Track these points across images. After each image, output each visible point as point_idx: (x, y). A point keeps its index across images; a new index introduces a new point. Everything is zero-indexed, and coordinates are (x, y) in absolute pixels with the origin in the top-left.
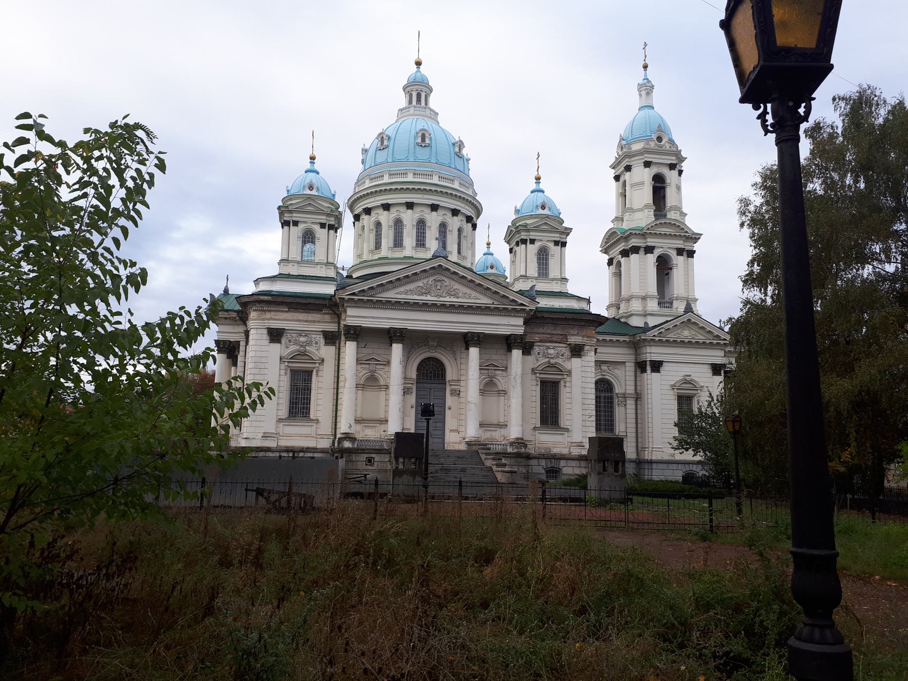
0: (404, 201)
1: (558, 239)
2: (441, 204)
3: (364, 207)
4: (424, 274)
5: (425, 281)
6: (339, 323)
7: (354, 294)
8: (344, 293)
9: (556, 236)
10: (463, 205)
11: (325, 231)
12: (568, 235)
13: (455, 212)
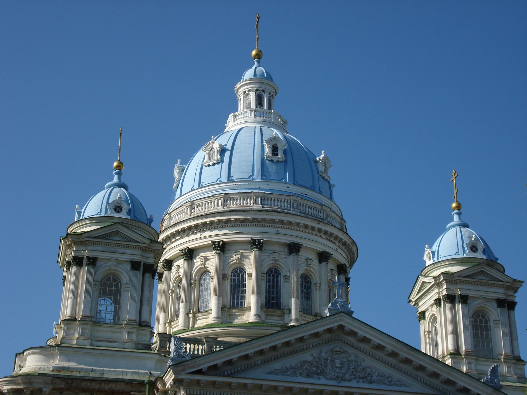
1: (502, 297)
4: (316, 340)
5: (315, 352)
7: (199, 372)
8: (183, 370)
9: (499, 293)
10: (335, 247)
11: (138, 275)
12: (516, 291)
13: (323, 257)
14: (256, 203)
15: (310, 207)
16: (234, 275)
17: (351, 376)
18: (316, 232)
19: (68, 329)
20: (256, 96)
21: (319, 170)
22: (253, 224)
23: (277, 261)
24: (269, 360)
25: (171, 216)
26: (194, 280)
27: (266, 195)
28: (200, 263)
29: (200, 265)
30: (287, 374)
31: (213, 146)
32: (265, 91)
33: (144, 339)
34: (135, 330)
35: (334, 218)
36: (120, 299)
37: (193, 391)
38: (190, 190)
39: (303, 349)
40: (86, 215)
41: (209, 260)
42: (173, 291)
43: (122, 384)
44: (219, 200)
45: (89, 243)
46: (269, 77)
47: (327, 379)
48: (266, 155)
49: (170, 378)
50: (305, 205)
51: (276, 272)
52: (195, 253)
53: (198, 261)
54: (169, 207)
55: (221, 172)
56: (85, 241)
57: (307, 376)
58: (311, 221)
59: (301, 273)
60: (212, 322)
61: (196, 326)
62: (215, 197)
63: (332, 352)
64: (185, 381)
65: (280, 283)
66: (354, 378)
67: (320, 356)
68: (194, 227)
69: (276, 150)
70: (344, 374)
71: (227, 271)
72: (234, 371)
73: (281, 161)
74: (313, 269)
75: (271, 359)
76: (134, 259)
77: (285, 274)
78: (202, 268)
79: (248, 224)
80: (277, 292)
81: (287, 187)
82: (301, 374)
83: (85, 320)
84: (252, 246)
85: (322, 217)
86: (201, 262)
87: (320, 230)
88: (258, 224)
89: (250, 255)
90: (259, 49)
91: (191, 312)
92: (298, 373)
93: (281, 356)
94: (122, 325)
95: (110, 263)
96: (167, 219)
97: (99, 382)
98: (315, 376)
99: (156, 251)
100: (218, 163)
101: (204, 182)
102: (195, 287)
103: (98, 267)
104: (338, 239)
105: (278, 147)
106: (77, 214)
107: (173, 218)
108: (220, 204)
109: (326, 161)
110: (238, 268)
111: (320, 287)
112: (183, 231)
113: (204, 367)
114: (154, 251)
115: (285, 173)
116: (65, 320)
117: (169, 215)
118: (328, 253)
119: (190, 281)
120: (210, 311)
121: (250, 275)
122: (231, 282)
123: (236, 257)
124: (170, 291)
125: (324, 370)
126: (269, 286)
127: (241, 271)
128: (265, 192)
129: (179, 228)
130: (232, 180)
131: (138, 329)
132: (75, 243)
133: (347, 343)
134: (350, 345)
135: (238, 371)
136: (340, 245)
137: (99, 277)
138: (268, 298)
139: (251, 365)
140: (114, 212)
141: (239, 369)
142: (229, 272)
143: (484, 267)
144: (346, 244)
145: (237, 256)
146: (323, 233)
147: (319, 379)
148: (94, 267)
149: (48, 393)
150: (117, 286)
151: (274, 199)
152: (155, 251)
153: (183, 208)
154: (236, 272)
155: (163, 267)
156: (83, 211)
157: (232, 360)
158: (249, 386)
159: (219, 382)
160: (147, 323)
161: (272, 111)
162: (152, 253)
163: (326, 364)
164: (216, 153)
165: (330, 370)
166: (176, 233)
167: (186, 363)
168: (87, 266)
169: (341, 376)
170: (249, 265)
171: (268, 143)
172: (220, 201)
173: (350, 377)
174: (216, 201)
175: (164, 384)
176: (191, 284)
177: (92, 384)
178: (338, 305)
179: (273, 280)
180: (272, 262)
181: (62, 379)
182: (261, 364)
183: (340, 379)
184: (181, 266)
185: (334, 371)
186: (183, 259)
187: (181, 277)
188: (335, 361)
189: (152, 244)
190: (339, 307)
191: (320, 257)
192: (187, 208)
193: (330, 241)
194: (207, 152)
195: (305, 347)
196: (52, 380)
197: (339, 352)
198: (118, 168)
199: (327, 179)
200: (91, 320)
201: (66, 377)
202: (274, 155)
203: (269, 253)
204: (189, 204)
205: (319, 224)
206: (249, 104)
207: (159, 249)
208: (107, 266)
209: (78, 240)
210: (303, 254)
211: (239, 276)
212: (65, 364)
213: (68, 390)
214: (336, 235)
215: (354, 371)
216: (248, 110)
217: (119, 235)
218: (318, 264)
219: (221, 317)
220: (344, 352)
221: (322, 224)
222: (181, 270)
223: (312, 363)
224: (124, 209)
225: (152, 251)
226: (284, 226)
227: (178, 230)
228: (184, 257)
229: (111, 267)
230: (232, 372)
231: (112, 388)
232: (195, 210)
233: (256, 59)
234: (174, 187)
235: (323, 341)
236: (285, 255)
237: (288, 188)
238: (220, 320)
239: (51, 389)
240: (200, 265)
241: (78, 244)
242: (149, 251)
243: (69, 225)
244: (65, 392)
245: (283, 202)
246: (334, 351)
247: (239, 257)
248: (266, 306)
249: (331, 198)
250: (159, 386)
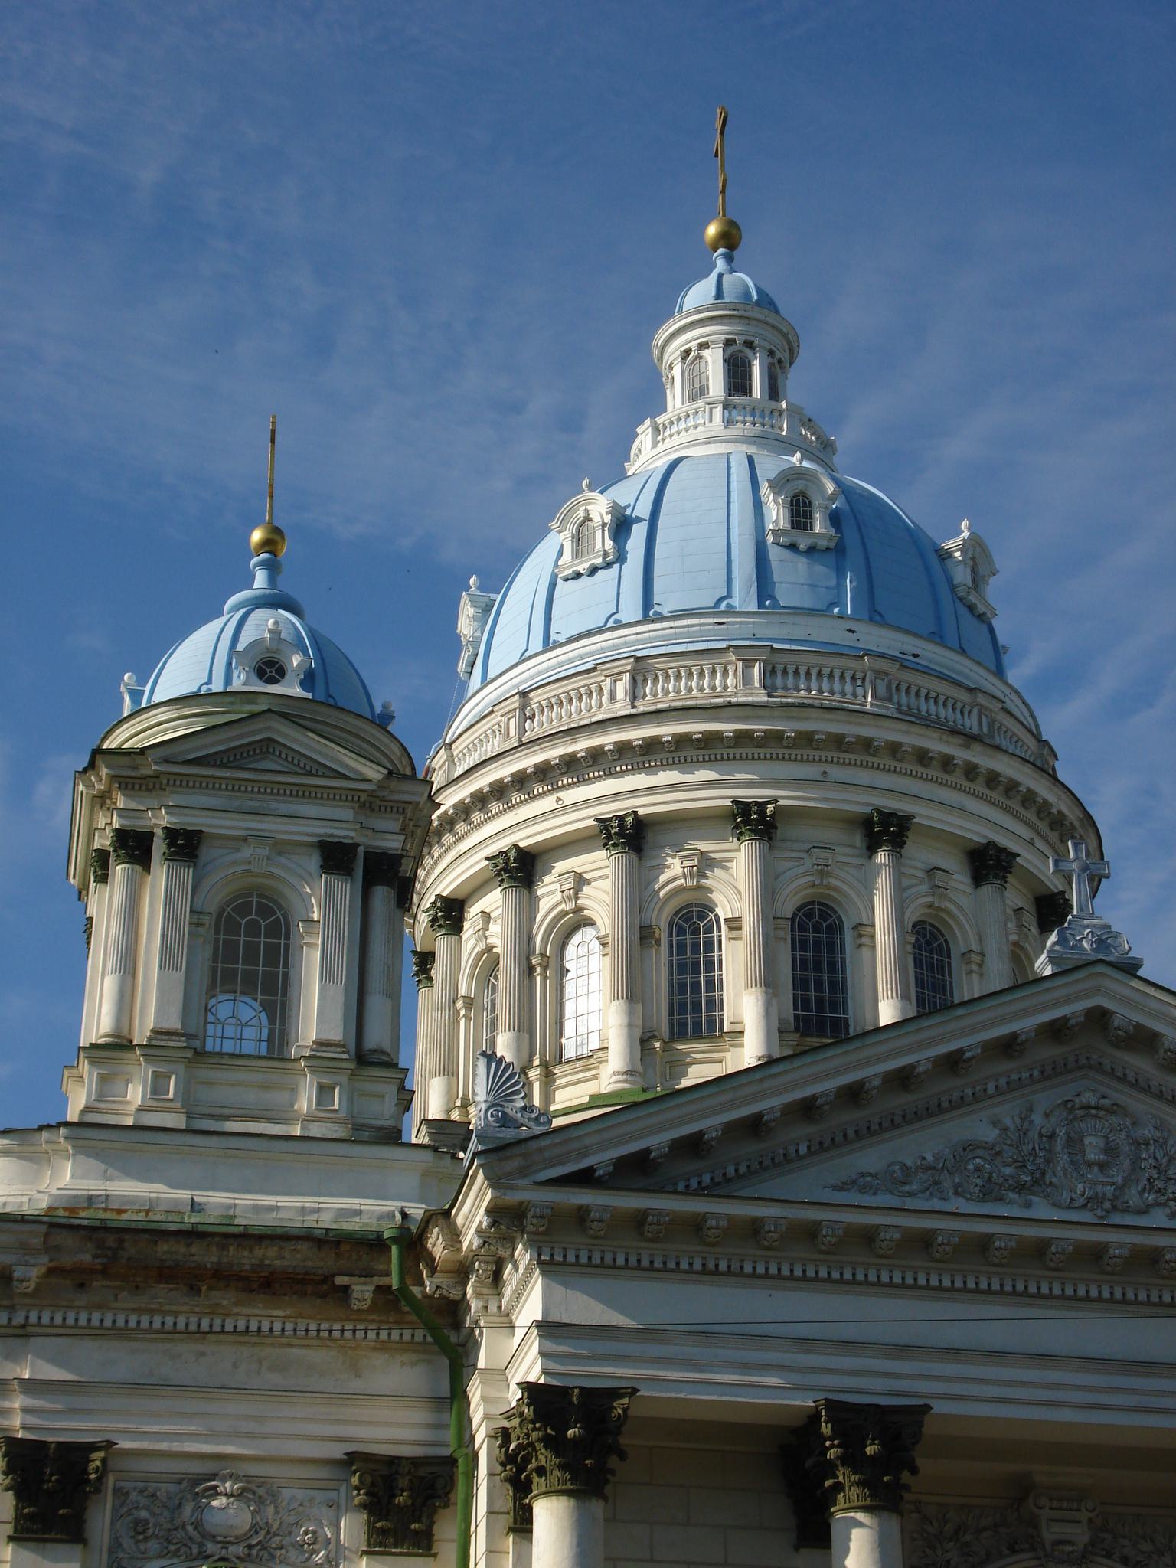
0: (720, 799)
2: (924, 815)
3: (493, 849)
5: (1008, 1112)
6: (458, 1396)
7: (584, 1178)
8: (523, 1172)
14: (746, 681)
15: (933, 694)
16: (681, 931)
17: (1146, 1195)
19: (103, 1079)
20: (725, 361)
21: (955, 582)
22: (738, 751)
23: (828, 874)
24: (839, 1138)
25: (455, 753)
26: (543, 955)
27: (777, 657)
28: (558, 897)
29: (559, 904)
30: (907, 1188)
31: (587, 511)
32: (755, 344)
33: (382, 1110)
34: (344, 1079)
35: (1016, 739)
36: (286, 975)
37: (565, 1249)
38: (517, 660)
39: (962, 1098)
40: (157, 698)
41: (588, 882)
42: (469, 1002)
43: (303, 1247)
44: (615, 681)
45: (171, 782)
46: (766, 302)
47: (1056, 1205)
48: (771, 527)
49: (474, 1208)
50: (914, 690)
51: (824, 915)
52: (539, 866)
53: (553, 892)
54: (446, 729)
55: (618, 594)
56: (157, 776)
57: (984, 1195)
59: (914, 919)
60: (610, 1086)
61: (553, 1108)
62: (601, 670)
63: (1071, 1110)
64: (531, 1213)
65: (843, 952)
66: (1159, 1205)
67: (1026, 1125)
68: (535, 773)
69: (805, 512)
70: (1121, 1188)
71: (654, 916)
72: (712, 1179)
73: (824, 548)
75: (845, 1135)
76: (331, 836)
77: (855, 921)
78: (567, 913)
79: (719, 751)
80: (833, 986)
81: (849, 630)
82: (959, 1189)
83: (162, 1043)
84: (737, 827)
85: (975, 730)
86: (563, 892)
87: (971, 771)
88: (756, 751)
89: (731, 860)
90: (732, 215)
91: (536, 1062)
92: (947, 1184)
93: (880, 1124)
94: (297, 1060)
95: (247, 852)
96: (440, 768)
97: (217, 1239)
98: (1012, 1195)
99: (409, 810)
100: (608, 565)
101: (561, 629)
102: (545, 978)
103: (204, 866)
104: (1035, 802)
105: (810, 502)
106: (127, 699)
107: (459, 759)
108: (620, 694)
109: (976, 549)
110: (690, 905)
111: (980, 965)
112: (498, 791)
113: (601, 1159)
114: (400, 808)
115: (841, 576)
116: (94, 1046)
117: (448, 751)
118: (1005, 849)
119: (529, 961)
120: (601, 1054)
121: (734, 924)
122: (671, 954)
123: (684, 868)
124: (460, 1004)
125: (1043, 1174)
126: (804, 963)
127: (702, 916)
128: (775, 646)
129: (482, 781)
130: (657, 613)
131: (352, 1075)
132: (126, 783)
133: (1123, 1079)
134: (1135, 1085)
135: (729, 1181)
136: (1043, 826)
137: (213, 900)
138: (801, 1003)
139: (773, 1159)
140: (254, 678)
141: (731, 1171)
142: (661, 922)
144: (1062, 825)
145: (686, 863)
146: (981, 780)
147: (1028, 1205)
148: (192, 864)
149: (33, 1285)
150: (274, 930)
151: (808, 670)
152: (404, 809)
153: (492, 719)
154: (686, 921)
155: (432, 927)
156: (148, 689)
157: (704, 1134)
158: (772, 1228)
159: (660, 1212)
160: (387, 1054)
161: (784, 405)
162: (398, 816)
163: (1050, 1151)
164: (599, 533)
165: (1065, 1171)
166: (473, 803)
167: (533, 1145)
168: (166, 859)
169: (1109, 1196)
170: (731, 893)
171: (776, 490)
172: (621, 687)
173: (1142, 1198)
174: (607, 686)
175: (454, 1236)
176: (531, 969)
177: (193, 1250)
178: (1081, 939)
179: (817, 944)
180: (810, 879)
181: (83, 1232)
182: (811, 1152)
183: (1107, 1205)
184: (493, 915)
185: (1083, 1175)
186: (500, 889)
187: (494, 950)
188: (1082, 1140)
189: (394, 784)
190: (1085, 944)
191: (977, 864)
192: (509, 719)
193: (1007, 810)
194: (567, 533)
195: (969, 1091)
196: (47, 1235)
197: (1096, 1108)
198: (267, 549)
199: (984, 614)
200: (185, 1044)
201: (98, 1223)
202: (798, 528)
203: (799, 851)
204: (516, 702)
205: (969, 748)
206: (703, 390)
207: (418, 800)
208: (234, 863)
209: (133, 774)
210: (919, 853)
211: (696, 931)
212: (94, 1185)
213: (104, 1272)
214: (1029, 790)
215: (1158, 1178)
216: (701, 403)
217: (277, 753)
219: (642, 1071)
220: (1115, 1109)
221: (977, 747)
222: (496, 928)
223: (997, 1150)
224: (289, 672)
225: (395, 809)
226: (847, 756)
227: (480, 791)
228: (502, 881)
229: (249, 863)
230: (704, 1185)
231: (267, 1262)
232: (535, 721)
233: (721, 251)
234: (461, 667)
235: (1032, 1069)
236: (852, 856)
237: (853, 632)
238: (638, 1079)
239: (43, 1270)
240: (559, 904)
241: (133, 788)
242: (383, 809)
243: (102, 735)
244: (95, 1284)
245: (837, 679)
246: (1077, 1106)
247: (693, 867)
248: (797, 1030)
249: (999, 672)
250: (436, 1244)
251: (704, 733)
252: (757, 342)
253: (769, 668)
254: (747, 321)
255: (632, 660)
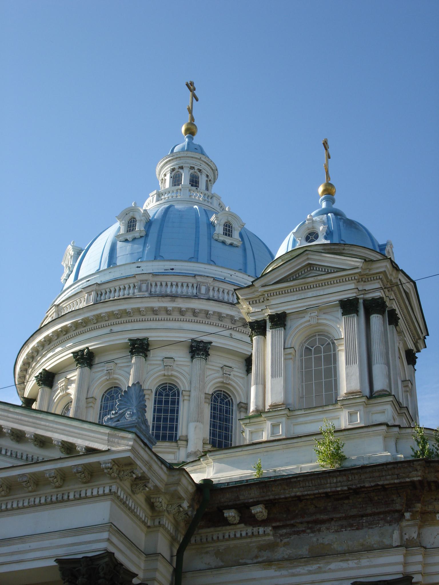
2: (153, 336)
18: (176, 315)
58: (159, 301)
74: (177, 371)
81: (138, 267)
143: (309, 256)
171: (121, 220)
180: (105, 377)
205: (174, 301)
218: (189, 364)
237: (139, 267)
251: (61, 328)
252: (184, 165)
253: (99, 293)
254: (179, 159)
255: (54, 307)
